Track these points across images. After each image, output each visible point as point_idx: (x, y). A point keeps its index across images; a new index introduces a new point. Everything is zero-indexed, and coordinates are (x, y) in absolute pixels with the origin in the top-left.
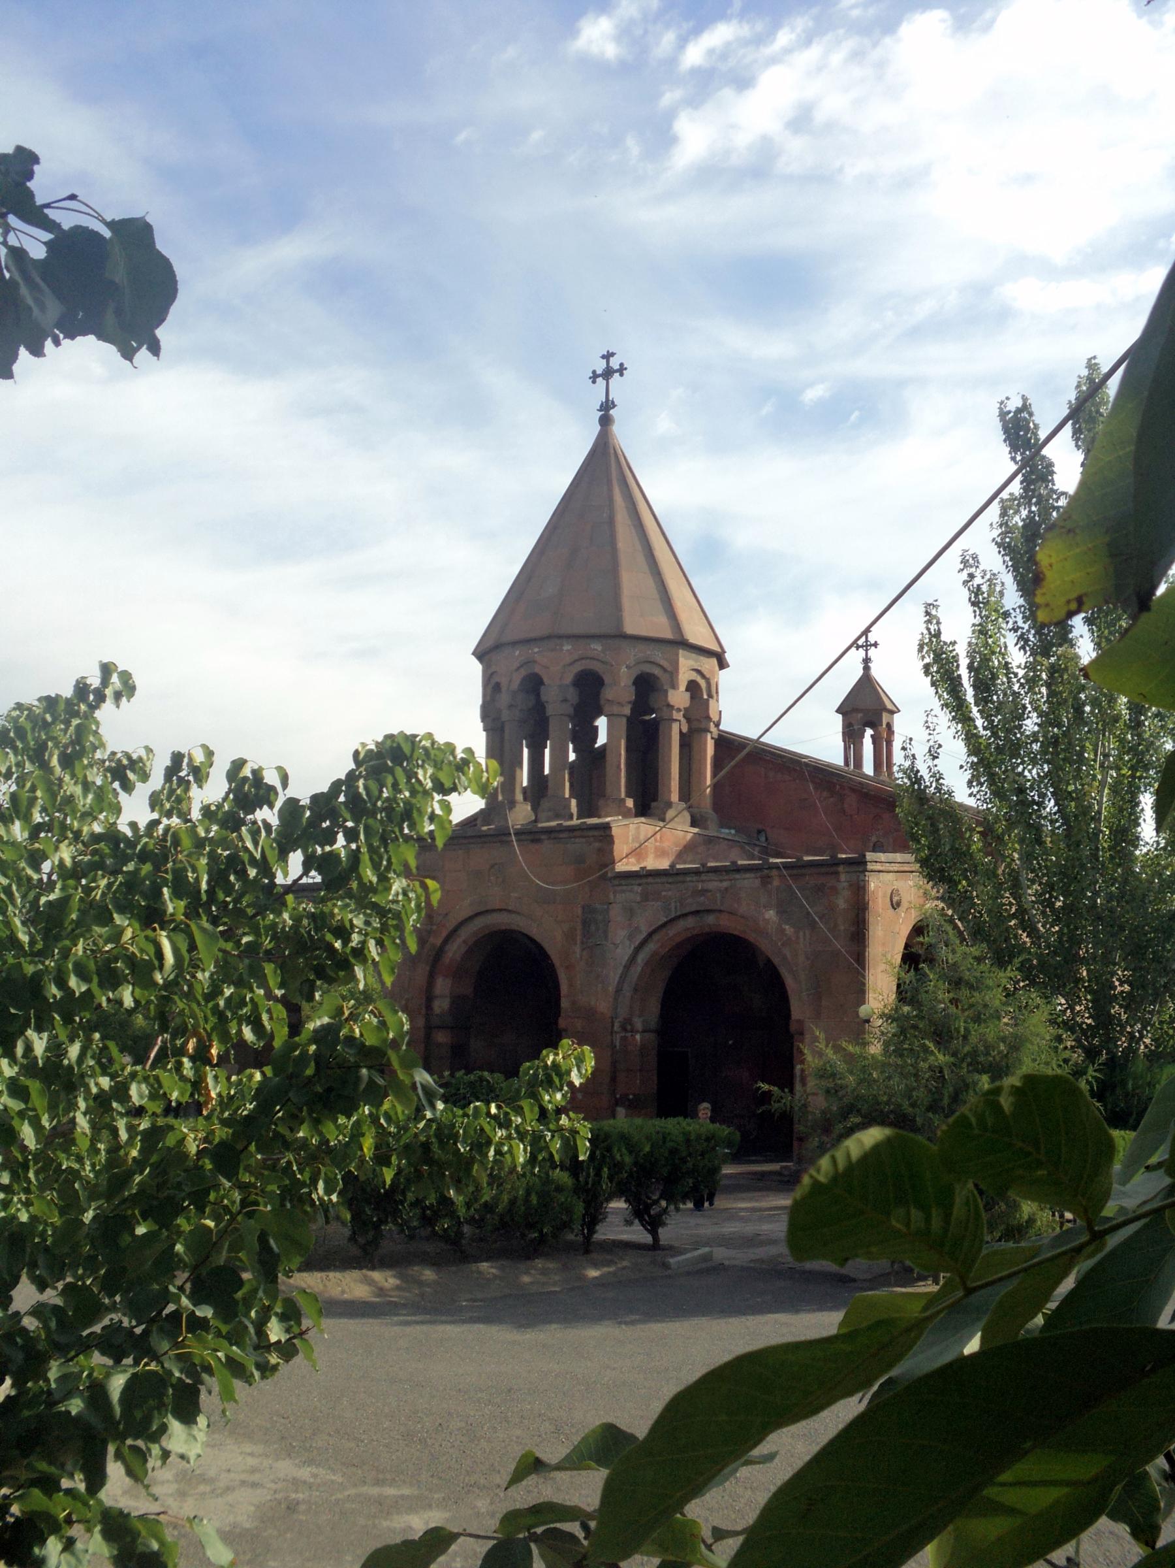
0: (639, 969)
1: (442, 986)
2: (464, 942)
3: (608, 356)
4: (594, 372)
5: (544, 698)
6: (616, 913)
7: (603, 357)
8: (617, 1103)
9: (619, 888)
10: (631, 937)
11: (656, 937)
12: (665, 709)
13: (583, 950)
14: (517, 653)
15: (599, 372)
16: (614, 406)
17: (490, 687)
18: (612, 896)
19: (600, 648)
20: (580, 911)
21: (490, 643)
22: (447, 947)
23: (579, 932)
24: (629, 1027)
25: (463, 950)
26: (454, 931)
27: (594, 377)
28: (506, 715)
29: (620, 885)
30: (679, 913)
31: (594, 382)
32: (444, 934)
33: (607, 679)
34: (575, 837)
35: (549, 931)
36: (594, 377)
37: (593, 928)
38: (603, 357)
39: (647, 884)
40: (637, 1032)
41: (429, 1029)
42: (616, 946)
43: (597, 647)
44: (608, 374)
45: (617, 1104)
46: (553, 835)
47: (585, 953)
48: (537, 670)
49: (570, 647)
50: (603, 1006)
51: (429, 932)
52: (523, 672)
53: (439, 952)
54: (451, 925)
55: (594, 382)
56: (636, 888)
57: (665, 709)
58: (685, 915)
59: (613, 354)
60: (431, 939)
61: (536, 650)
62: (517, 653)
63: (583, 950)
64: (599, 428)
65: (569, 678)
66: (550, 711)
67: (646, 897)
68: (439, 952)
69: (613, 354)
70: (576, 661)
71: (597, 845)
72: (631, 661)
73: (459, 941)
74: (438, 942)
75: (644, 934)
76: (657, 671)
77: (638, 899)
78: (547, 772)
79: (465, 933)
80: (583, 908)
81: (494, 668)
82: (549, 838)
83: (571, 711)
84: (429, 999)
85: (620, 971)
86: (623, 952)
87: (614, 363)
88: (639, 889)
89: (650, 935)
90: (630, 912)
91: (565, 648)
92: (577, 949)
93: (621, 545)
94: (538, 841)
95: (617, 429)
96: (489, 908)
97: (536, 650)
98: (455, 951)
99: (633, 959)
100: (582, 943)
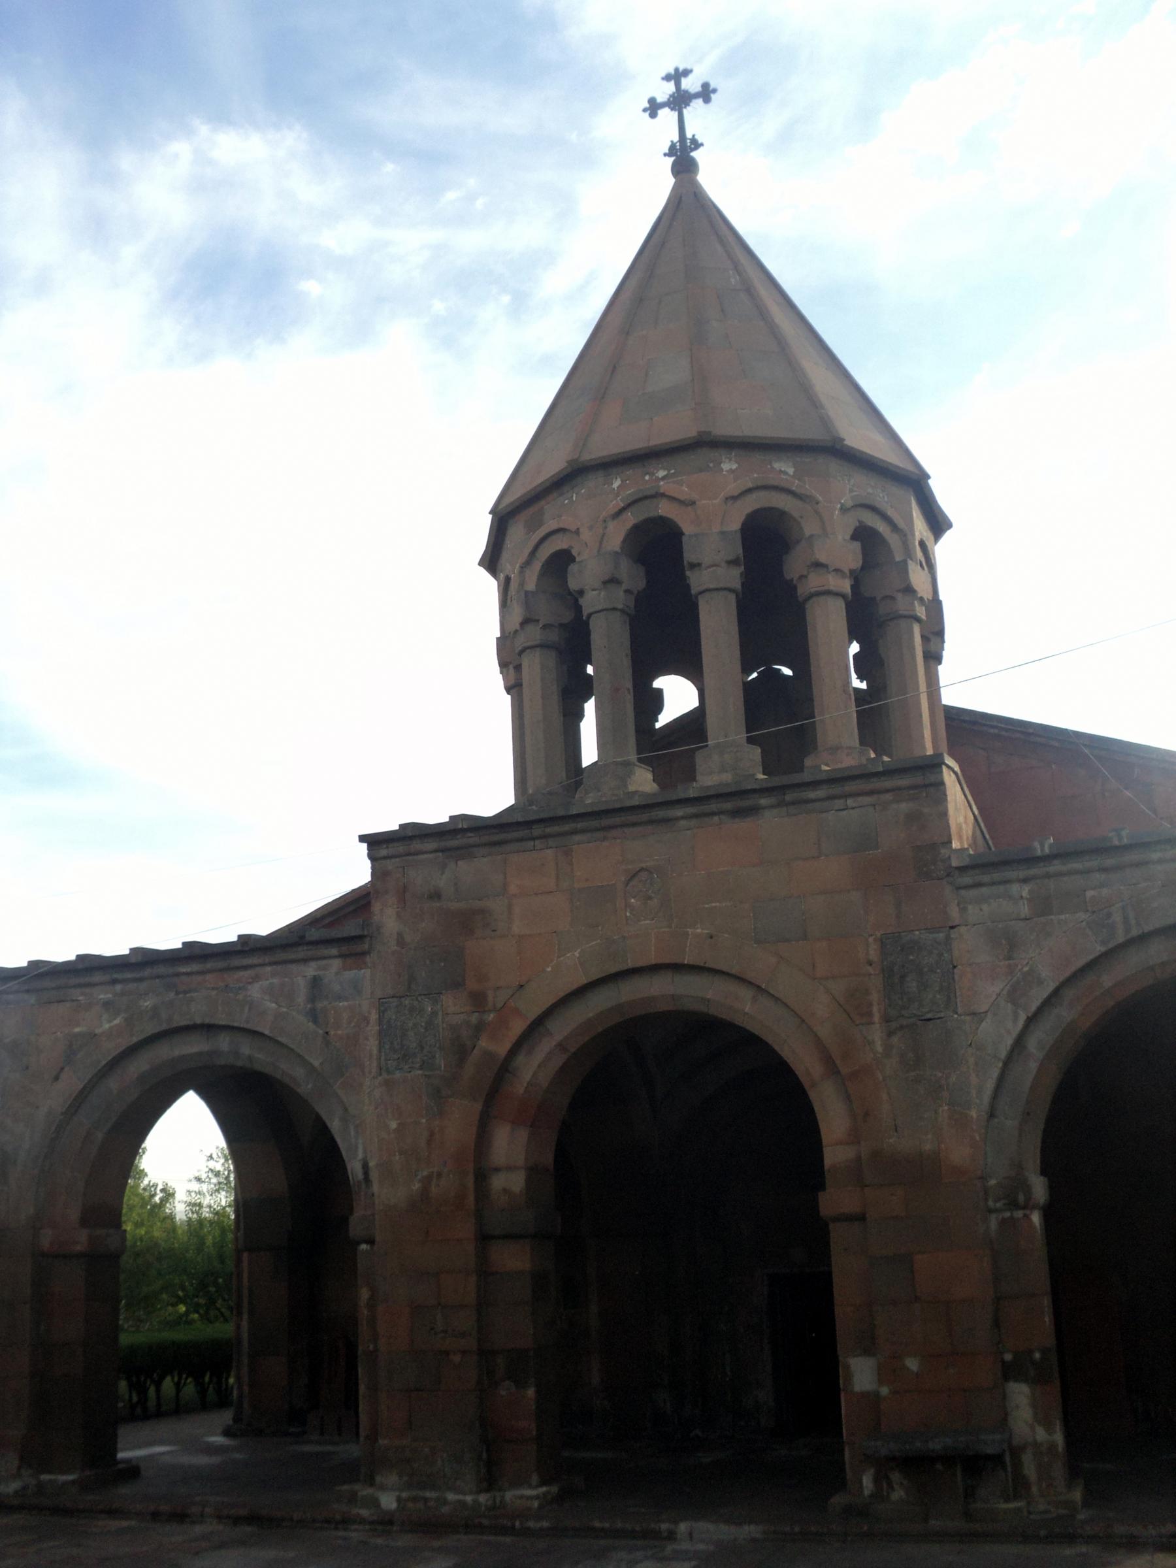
0: (1033, 1066)
1: (510, 1146)
2: (561, 1046)
3: (677, 76)
4: (652, 101)
5: (689, 556)
6: (970, 946)
7: (668, 78)
8: (1010, 1372)
9: (973, 893)
10: (1014, 995)
11: (1069, 994)
12: (899, 596)
13: (890, 1034)
14: (616, 484)
15: (661, 98)
16: (696, 145)
17: (537, 566)
18: (954, 912)
19: (791, 471)
20: (873, 953)
21: (555, 465)
22: (520, 1059)
23: (875, 997)
24: (1021, 1198)
25: (558, 1061)
26: (539, 1023)
27: (653, 108)
28: (591, 601)
29: (979, 885)
30: (1135, 932)
31: (653, 115)
32: (518, 1027)
33: (809, 528)
34: (845, 796)
35: (793, 1006)
36: (653, 108)
37: (912, 985)
38: (668, 78)
39: (1048, 876)
40: (1034, 1208)
41: (484, 1238)
42: (978, 1017)
43: (784, 468)
44: (679, 101)
45: (1006, 1377)
46: (789, 797)
47: (895, 1040)
48: (664, 509)
49: (734, 466)
50: (958, 1153)
51: (479, 1028)
52: (630, 519)
53: (504, 1069)
54: (533, 1004)
55: (653, 115)
56: (1015, 888)
57: (899, 596)
58: (1143, 938)
59: (687, 73)
60: (484, 1043)
61: (661, 473)
62: (616, 484)
63: (890, 1034)
64: (672, 180)
65: (735, 525)
66: (697, 581)
67: (1043, 906)
68: (504, 1069)
69: (687, 73)
70: (749, 491)
71: (904, 807)
72: (846, 500)
73: (544, 1047)
74: (502, 1049)
75: (1051, 987)
76: (882, 527)
77: (1025, 910)
78: (589, 754)
79: (562, 1028)
80: (882, 942)
81: (552, 525)
82: (778, 805)
83: (737, 584)
84: (482, 1176)
85: (995, 1073)
86: (997, 1030)
87: (690, 84)
88: (1025, 891)
89: (1056, 992)
90: (1007, 943)
91: (726, 466)
92: (876, 1035)
93: (777, 320)
94: (754, 811)
95: (704, 178)
96: (630, 964)
97: (661, 473)
98: (535, 1069)
99: (1019, 1043)
100: (887, 1019)
